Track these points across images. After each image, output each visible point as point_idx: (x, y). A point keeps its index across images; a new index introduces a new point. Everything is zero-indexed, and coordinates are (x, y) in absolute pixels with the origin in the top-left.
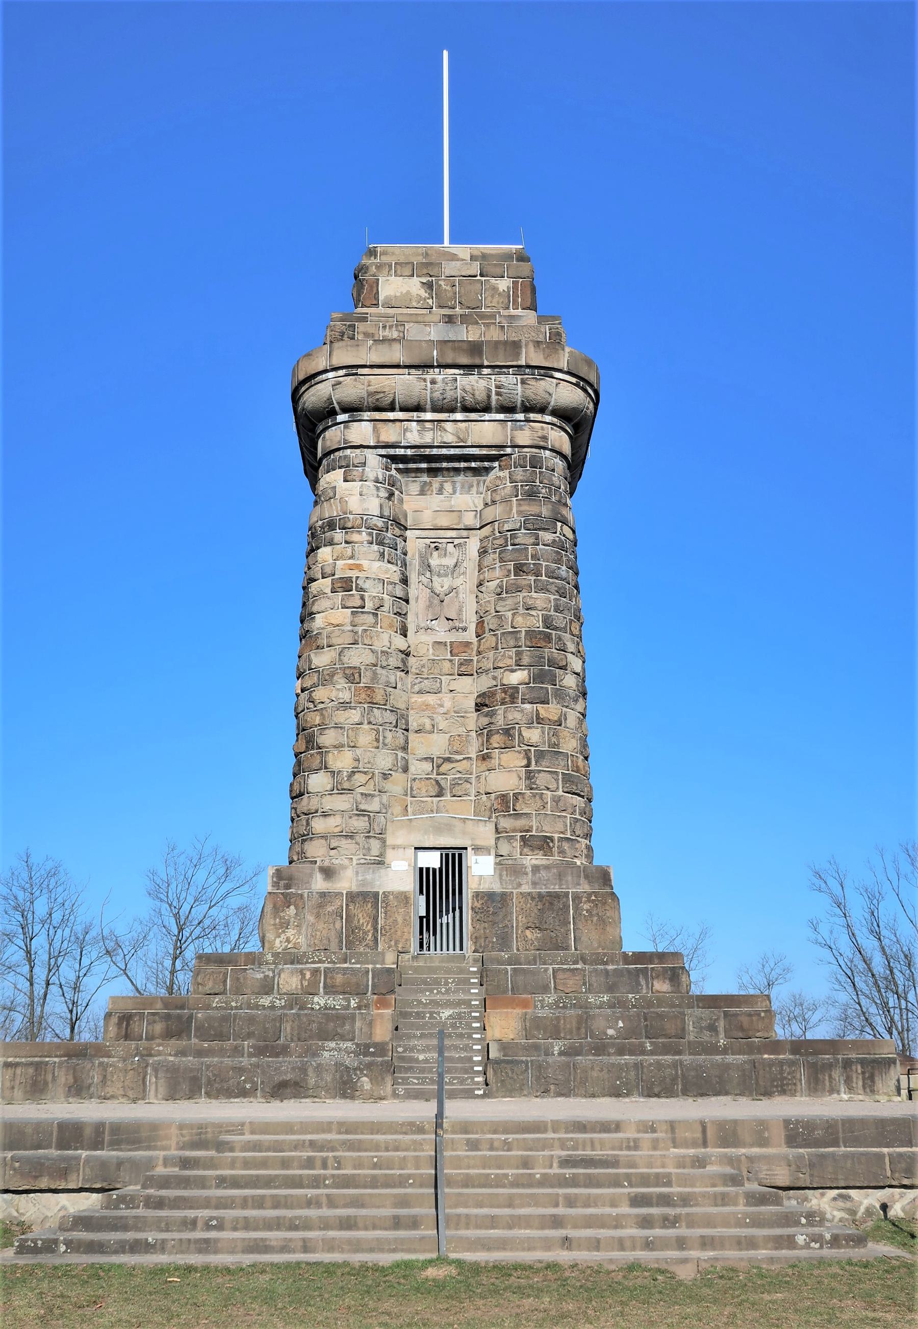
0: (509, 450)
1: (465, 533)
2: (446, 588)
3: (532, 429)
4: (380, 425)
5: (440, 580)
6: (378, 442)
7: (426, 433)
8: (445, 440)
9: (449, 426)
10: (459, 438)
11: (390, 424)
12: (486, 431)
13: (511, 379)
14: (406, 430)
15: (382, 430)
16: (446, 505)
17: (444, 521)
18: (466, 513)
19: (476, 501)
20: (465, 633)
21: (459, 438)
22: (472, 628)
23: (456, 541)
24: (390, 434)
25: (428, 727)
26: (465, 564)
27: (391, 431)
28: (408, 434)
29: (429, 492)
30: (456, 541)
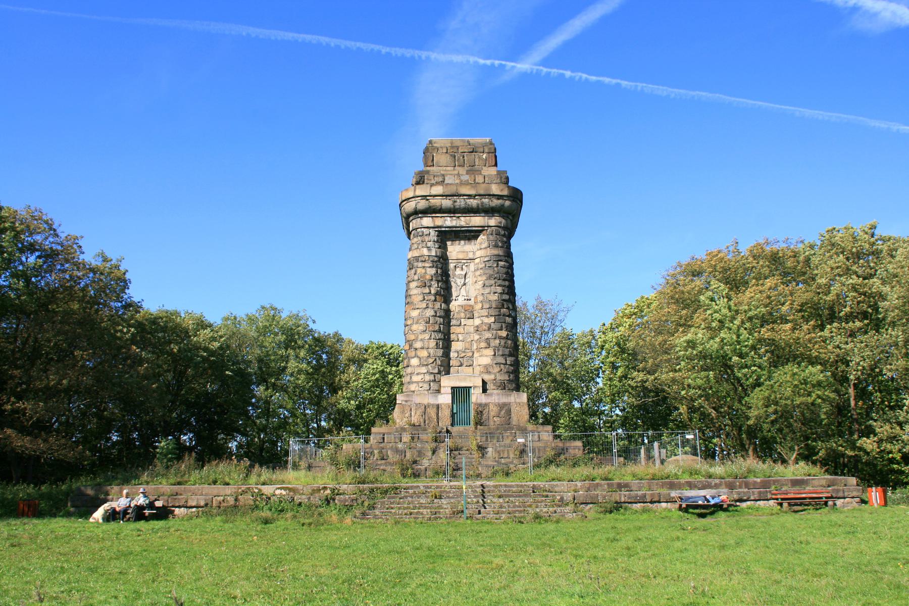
9: (462, 218)
12: (477, 221)
13: (487, 200)
16: (462, 249)
17: (461, 257)
24: (439, 222)
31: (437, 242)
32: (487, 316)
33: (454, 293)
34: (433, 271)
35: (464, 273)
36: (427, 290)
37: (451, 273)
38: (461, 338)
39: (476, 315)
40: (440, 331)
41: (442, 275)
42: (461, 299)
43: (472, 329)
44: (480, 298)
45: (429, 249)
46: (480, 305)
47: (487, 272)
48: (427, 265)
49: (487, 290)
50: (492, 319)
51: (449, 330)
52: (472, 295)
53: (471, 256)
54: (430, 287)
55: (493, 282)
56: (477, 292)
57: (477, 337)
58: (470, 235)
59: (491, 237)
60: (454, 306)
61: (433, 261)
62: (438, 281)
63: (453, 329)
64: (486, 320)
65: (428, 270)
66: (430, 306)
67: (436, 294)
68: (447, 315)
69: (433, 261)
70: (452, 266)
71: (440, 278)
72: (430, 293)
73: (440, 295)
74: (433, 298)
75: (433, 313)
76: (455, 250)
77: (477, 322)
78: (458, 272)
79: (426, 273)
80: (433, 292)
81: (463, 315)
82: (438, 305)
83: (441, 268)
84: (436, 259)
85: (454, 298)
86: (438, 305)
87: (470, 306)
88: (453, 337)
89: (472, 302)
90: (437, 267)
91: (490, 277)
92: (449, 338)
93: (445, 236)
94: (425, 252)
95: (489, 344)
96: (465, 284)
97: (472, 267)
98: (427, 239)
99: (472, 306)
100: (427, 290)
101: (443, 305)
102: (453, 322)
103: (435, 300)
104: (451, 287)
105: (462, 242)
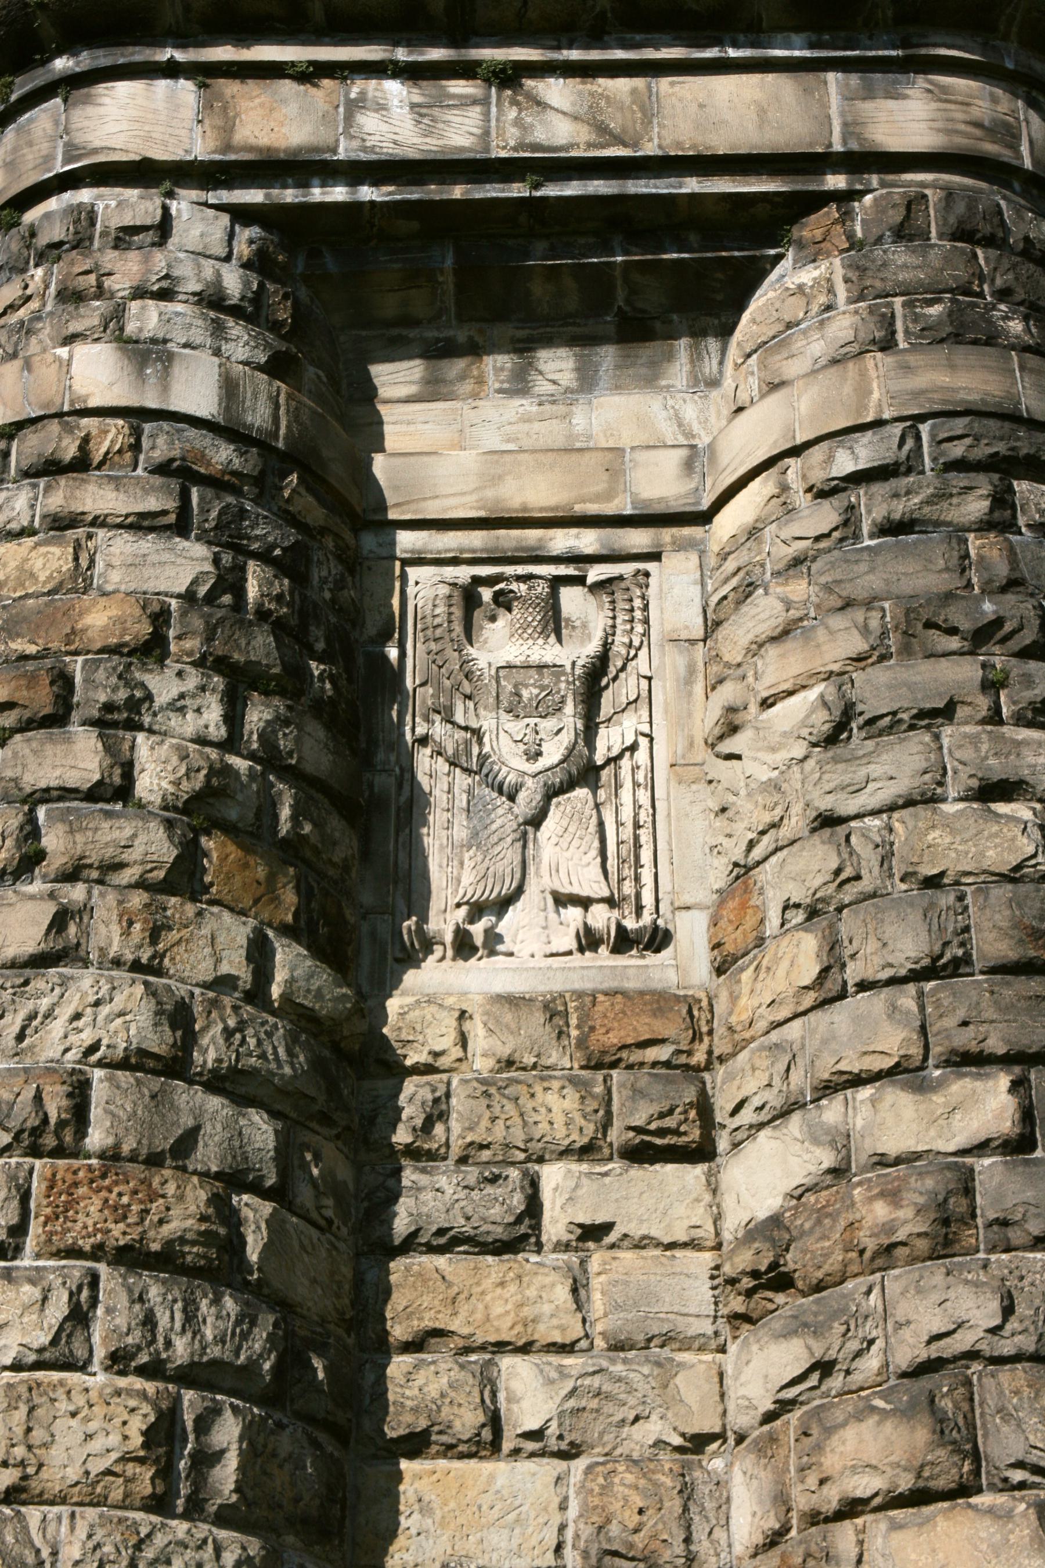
0: (836, 182)
1: (638, 539)
2: (553, 753)
3: (942, 95)
4: (230, 87)
5: (517, 727)
6: (228, 148)
7: (454, 117)
8: (540, 135)
9: (555, 91)
10: (601, 129)
11: (287, 87)
14: (354, 106)
15: (244, 104)
16: (549, 432)
17: (538, 493)
18: (642, 456)
19: (690, 412)
20: (652, 959)
21: (601, 129)
22: (692, 934)
23: (595, 573)
24: (278, 119)
25: (467, 1420)
26: (641, 664)
27: (292, 109)
28: (369, 122)
29: (468, 386)
30: (595, 573)
31: (251, 311)
32: (903, 1073)
33: (451, 871)
34: (181, 566)
35: (574, 653)
36: (81, 758)
37: (412, 658)
38: (530, 1395)
39: (742, 1083)
40: (212, 1262)
41: (290, 630)
42: (535, 946)
43: (689, 1292)
44: (802, 871)
45: (147, 354)
46: (800, 957)
47: (868, 581)
48: (96, 497)
49: (894, 766)
50: (988, 1105)
51: (369, 1299)
52: (686, 878)
53: (660, 482)
54: (120, 720)
55: (962, 673)
56: (753, 815)
57: (764, 1365)
58: (654, 270)
59: (901, 261)
60: (430, 1003)
61: (178, 472)
62: (239, 684)
63: (417, 1291)
64: (893, 1121)
65: (116, 550)
66: (107, 933)
67: (197, 812)
68: (344, 1089)
69: (178, 472)
70: (425, 589)
71: (260, 647)
72: (116, 790)
73: (254, 833)
74: (153, 846)
75: (129, 1018)
76: (456, 441)
77: (763, 1174)
78: (502, 644)
79: (80, 580)
80: (156, 773)
81: (558, 1111)
82: (214, 944)
83: (290, 565)
84: (223, 455)
85: (443, 920)
86: (214, 944)
87: (659, 1001)
88: (414, 1386)
89: (685, 963)
90: (229, 539)
91: (919, 626)
92: (361, 1392)
93: (375, 279)
94: (96, 373)
95: (962, 1438)
96: (583, 773)
97: (676, 591)
98: (125, 270)
99: (693, 1014)
100: (81, 758)
101: (289, 962)
102: (427, 1198)
103: (184, 878)
104: (412, 806)
105: (557, 365)
